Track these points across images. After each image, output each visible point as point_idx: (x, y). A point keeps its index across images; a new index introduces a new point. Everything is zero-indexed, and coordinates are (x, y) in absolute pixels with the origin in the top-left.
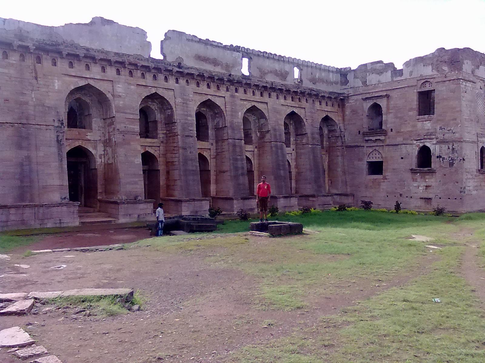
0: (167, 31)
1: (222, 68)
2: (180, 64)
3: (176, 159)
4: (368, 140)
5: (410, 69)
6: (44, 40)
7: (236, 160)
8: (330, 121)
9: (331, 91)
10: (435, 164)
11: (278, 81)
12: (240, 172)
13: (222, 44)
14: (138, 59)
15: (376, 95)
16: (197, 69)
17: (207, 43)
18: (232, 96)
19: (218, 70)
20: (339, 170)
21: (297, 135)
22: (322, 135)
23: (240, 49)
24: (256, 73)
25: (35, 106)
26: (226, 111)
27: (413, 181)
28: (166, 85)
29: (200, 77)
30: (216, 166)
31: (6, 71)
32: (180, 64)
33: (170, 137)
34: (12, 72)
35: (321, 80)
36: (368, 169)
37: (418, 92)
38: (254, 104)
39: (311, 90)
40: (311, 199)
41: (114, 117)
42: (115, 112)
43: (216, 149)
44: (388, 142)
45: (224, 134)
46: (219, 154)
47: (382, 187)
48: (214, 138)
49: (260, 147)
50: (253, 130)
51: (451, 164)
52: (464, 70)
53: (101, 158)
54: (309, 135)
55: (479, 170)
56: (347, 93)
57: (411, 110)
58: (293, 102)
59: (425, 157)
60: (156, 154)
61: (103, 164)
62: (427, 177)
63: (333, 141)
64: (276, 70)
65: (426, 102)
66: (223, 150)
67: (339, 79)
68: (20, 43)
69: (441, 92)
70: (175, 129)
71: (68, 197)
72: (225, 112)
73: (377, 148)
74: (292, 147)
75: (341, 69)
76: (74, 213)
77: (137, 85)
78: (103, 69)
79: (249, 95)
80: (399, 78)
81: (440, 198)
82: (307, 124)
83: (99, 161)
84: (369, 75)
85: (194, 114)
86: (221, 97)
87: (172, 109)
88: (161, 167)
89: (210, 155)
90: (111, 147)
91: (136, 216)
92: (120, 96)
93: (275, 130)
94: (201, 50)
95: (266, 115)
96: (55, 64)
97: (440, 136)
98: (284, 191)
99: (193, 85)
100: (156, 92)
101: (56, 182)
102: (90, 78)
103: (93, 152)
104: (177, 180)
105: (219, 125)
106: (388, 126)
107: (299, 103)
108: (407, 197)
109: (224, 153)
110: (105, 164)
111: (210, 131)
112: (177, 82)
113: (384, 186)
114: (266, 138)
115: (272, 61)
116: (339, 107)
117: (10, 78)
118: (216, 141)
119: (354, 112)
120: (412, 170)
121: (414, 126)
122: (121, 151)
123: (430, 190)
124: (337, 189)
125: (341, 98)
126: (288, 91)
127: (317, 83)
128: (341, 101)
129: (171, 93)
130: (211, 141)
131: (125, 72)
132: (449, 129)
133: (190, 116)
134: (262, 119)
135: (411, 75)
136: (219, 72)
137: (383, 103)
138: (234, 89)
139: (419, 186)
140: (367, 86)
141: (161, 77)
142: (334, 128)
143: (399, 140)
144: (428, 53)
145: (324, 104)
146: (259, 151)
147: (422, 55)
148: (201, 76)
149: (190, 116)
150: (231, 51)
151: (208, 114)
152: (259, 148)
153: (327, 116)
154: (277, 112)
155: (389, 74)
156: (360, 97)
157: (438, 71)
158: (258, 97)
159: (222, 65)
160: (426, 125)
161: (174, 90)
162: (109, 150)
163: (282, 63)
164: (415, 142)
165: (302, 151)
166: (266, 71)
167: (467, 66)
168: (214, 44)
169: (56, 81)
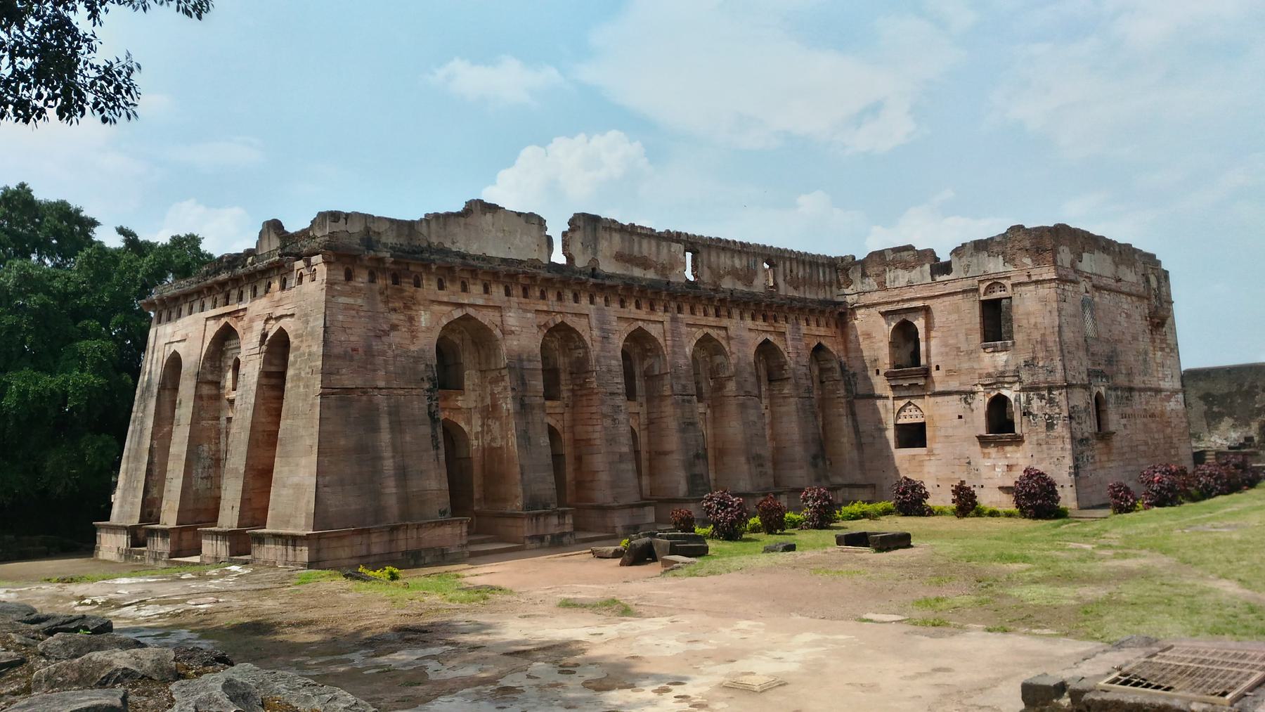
1: (656, 272)
2: (594, 269)
3: (597, 435)
11: (740, 287)
17: (631, 231)
18: (674, 320)
19: (651, 275)
20: (845, 440)
21: (770, 381)
24: (706, 277)
30: (649, 443)
32: (594, 269)
38: (706, 330)
39: (792, 299)
47: (926, 469)
53: (477, 438)
60: (559, 427)
71: (449, 510)
78: (486, 291)
80: (945, 277)
83: (475, 443)
85: (619, 354)
86: (658, 324)
88: (567, 450)
90: (498, 419)
92: (513, 332)
96: (418, 284)
103: (466, 429)
110: (484, 449)
112: (592, 302)
126: (758, 304)
129: (584, 321)
130: (639, 399)
132: (1041, 364)
140: (887, 289)
141: (569, 295)
143: (954, 385)
149: (615, 358)
154: (743, 343)
155: (927, 267)
158: (712, 320)
162: (495, 426)
165: (784, 409)
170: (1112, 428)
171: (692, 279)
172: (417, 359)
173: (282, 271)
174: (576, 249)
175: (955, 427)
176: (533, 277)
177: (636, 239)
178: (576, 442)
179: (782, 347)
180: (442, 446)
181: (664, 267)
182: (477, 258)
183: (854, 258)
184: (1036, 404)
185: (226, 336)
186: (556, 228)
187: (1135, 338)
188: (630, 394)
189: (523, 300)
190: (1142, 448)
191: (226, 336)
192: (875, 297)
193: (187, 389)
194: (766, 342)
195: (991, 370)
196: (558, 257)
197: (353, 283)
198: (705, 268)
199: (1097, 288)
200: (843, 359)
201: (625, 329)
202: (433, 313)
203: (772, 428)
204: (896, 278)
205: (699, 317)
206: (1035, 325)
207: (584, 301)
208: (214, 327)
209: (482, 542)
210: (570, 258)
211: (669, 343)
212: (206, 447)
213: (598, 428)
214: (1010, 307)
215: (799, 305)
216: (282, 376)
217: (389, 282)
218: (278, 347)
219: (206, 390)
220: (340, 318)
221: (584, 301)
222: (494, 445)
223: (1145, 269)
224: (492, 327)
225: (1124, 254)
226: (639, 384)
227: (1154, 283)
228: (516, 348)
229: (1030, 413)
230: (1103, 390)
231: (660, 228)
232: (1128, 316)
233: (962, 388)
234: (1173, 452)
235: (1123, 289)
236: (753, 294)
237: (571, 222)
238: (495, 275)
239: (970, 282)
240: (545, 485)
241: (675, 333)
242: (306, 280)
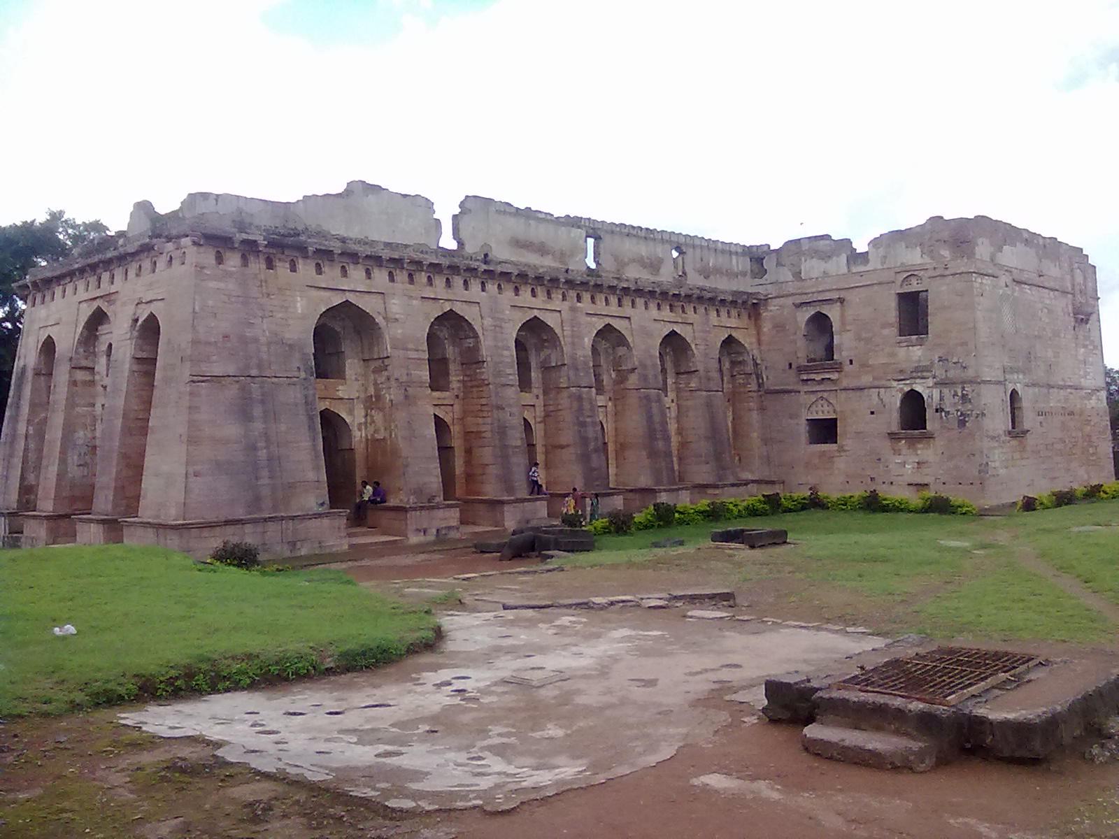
0: (463, 198)
2: (486, 255)
4: (807, 380)
5: (881, 251)
7: (583, 425)
8: (734, 345)
9: (735, 289)
12: (592, 446)
13: (552, 215)
14: (422, 252)
15: (820, 299)
17: (528, 214)
19: (545, 264)
22: (721, 370)
23: (583, 223)
25: (269, 344)
26: (564, 336)
28: (466, 295)
29: (520, 279)
31: (222, 285)
32: (486, 255)
33: (472, 387)
34: (231, 286)
35: (718, 271)
36: (809, 432)
37: (898, 293)
39: (702, 289)
40: (710, 491)
41: (388, 357)
42: (391, 348)
43: (544, 406)
44: (845, 383)
46: (552, 414)
48: (541, 386)
49: (619, 398)
50: (604, 366)
51: (962, 423)
52: (978, 256)
53: (360, 430)
54: (702, 372)
55: (1010, 433)
56: (765, 293)
57: (884, 326)
58: (673, 315)
59: (914, 411)
60: (448, 419)
61: (364, 440)
62: (920, 446)
63: (741, 381)
64: (642, 257)
65: (913, 313)
66: (560, 407)
67: (749, 267)
68: (244, 236)
69: (939, 295)
72: (561, 339)
73: (825, 395)
74: (672, 395)
75: (751, 246)
76: (339, 528)
77: (422, 298)
79: (600, 306)
80: (862, 268)
81: (944, 483)
82: (697, 350)
84: (806, 261)
87: (478, 337)
88: (457, 443)
89: (535, 417)
90: (381, 409)
91: (434, 531)
92: (397, 320)
93: (644, 366)
94: (517, 227)
95: (630, 340)
96: (293, 269)
97: (939, 372)
98: (665, 480)
99: (509, 293)
100: (451, 310)
101: (311, 476)
102: (349, 291)
104: (487, 465)
105: (550, 362)
106: (844, 354)
107: (684, 315)
108: (884, 483)
109: (560, 413)
110: (367, 440)
111: (533, 374)
113: (841, 464)
114: (630, 382)
115: (635, 240)
116: (750, 317)
117: (229, 296)
118: (544, 392)
119: (779, 327)
120: (889, 434)
121: (893, 355)
122: (401, 416)
123: (926, 471)
124: (752, 472)
125: (755, 301)
126: (664, 294)
127: (712, 277)
128: (752, 307)
129: (475, 309)
130: (535, 391)
131: (401, 276)
133: (508, 348)
134: (621, 348)
135: (883, 263)
136: (550, 267)
137: (833, 313)
138: (575, 295)
139: (905, 462)
141: (458, 281)
142: (741, 359)
143: (866, 379)
144: (913, 225)
145: (723, 313)
146: (615, 406)
147: (903, 228)
148: (523, 276)
149: (508, 348)
150: (568, 228)
151: (531, 342)
152: (616, 399)
153: (730, 336)
154: (648, 334)
155: (843, 258)
156: (790, 301)
157: (932, 258)
158: (614, 309)
160: (916, 353)
161: (478, 303)
163: (651, 244)
164: (895, 384)
165: (689, 403)
166: (626, 260)
167: (983, 249)
168: (540, 216)
169: (299, 299)
170: (1027, 426)
171: (593, 266)
173: (153, 253)
176: (419, 263)
177: (532, 222)
178: (467, 434)
181: (562, 254)
182: (359, 242)
183: (769, 246)
185: (98, 319)
186: (445, 211)
187: (1056, 334)
188: (525, 383)
190: (1059, 446)
191: (98, 319)
193: (62, 375)
194: (673, 333)
195: (903, 366)
196: (448, 242)
197: (221, 266)
199: (1019, 282)
200: (756, 352)
201: (522, 318)
203: (678, 422)
205: (600, 306)
207: (475, 286)
208: (87, 311)
209: (364, 534)
210: (461, 244)
212: (81, 433)
213: (489, 420)
214: (926, 300)
215: (709, 295)
216: (153, 361)
217: (264, 266)
218: (150, 330)
219: (81, 376)
220: (210, 303)
221: (475, 286)
223: (1071, 265)
225: (1050, 248)
226: (535, 375)
227: (1079, 278)
228: (399, 337)
229: (942, 410)
230: (1019, 387)
231: (558, 212)
232: (1050, 311)
233: (876, 383)
234: (1091, 450)
235: (1046, 285)
236: (659, 284)
237: (462, 205)
238: (377, 260)
240: (434, 481)
242: (176, 263)
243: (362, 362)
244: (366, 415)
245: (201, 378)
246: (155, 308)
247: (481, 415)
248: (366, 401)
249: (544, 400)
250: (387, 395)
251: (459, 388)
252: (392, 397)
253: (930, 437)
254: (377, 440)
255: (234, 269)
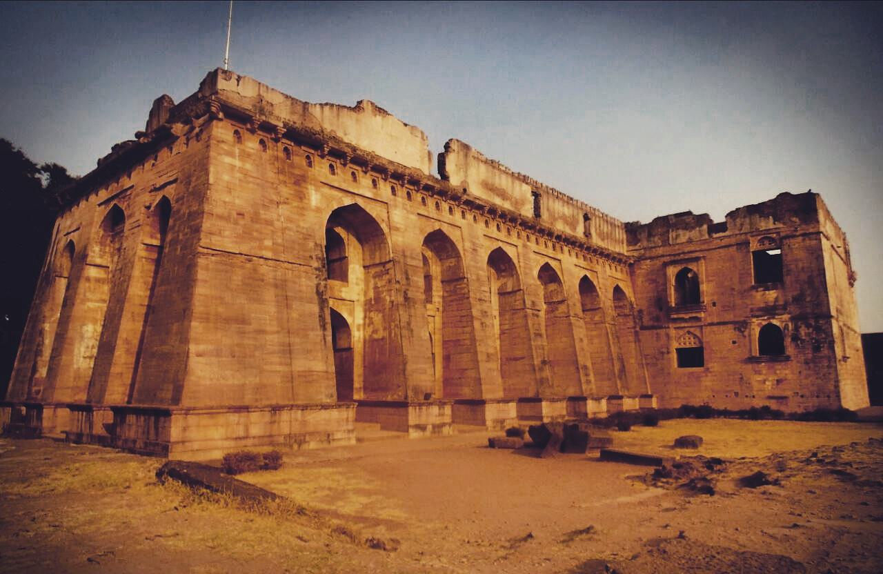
6: (295, 123)
10: (790, 350)
11: (568, 231)
16: (486, 202)
18: (525, 246)
19: (507, 206)
27: (756, 374)
44: (709, 320)
45: (515, 301)
51: (817, 349)
53: (359, 330)
70: (463, 288)
72: (518, 268)
77: (418, 214)
80: (721, 234)
87: (460, 256)
92: (397, 229)
104: (466, 369)
112: (464, 217)
115: (561, 203)
129: (458, 232)
132: (808, 299)
134: (553, 284)
144: (766, 200)
154: (571, 274)
155: (705, 227)
158: (550, 252)
159: (511, 200)
172: (307, 236)
174: (450, 167)
175: (729, 350)
179: (595, 283)
180: (329, 327)
181: (517, 203)
184: (803, 331)
189: (407, 202)
192: (660, 251)
195: (762, 305)
198: (545, 210)
200: (633, 299)
202: (323, 195)
204: (677, 236)
205: (542, 249)
206: (803, 268)
211: (522, 264)
222: (375, 336)
224: (379, 221)
231: (515, 170)
233: (736, 319)
239: (743, 237)
241: (527, 259)
243: (362, 268)
244: (365, 317)
245: (210, 251)
246: (170, 192)
247: (460, 324)
248: (365, 305)
249: (500, 321)
250: (388, 298)
251: (439, 303)
252: (393, 298)
253: (788, 358)
254: (377, 340)
255: (252, 151)
